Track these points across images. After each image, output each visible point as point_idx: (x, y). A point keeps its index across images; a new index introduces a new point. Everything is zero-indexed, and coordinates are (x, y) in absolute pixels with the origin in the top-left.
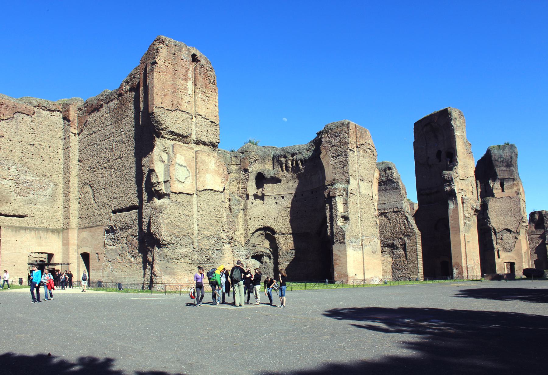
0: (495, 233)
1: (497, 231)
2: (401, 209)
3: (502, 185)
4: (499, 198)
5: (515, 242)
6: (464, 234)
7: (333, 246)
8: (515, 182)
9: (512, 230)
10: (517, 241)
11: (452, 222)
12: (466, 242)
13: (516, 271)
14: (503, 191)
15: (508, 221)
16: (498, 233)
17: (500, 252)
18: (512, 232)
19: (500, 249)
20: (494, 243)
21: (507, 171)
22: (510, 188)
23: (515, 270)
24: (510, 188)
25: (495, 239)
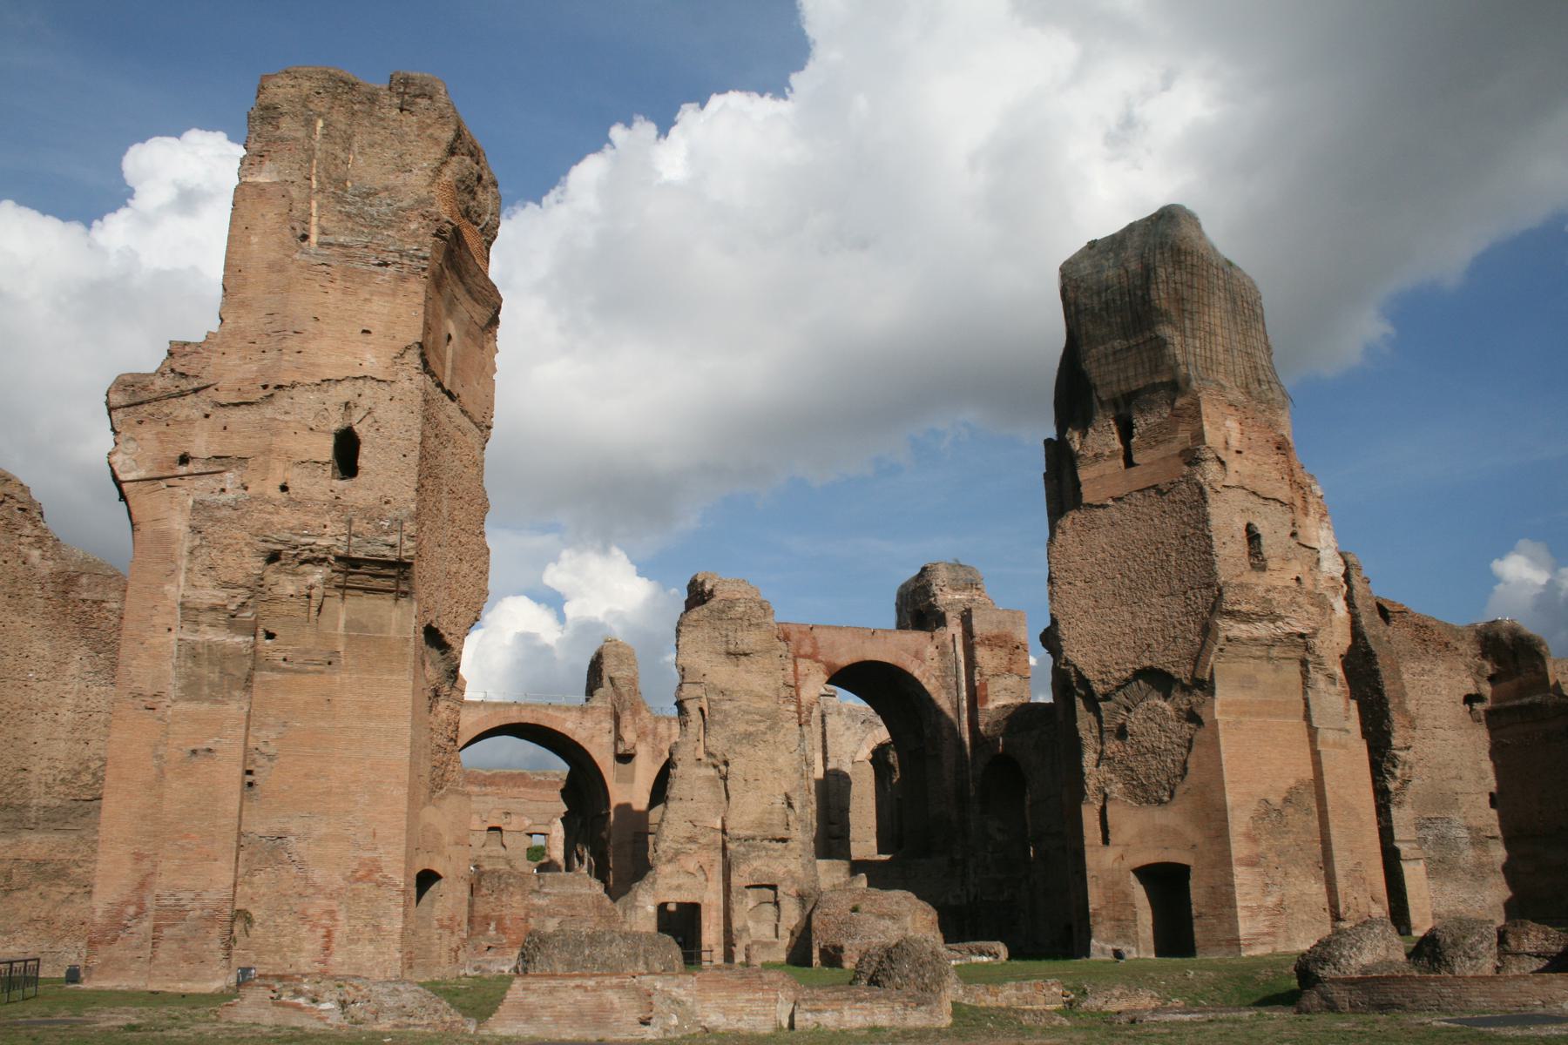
0: (1092, 703)
1: (1099, 688)
3: (1126, 432)
4: (1104, 506)
5: (1190, 741)
7: (566, 809)
9: (1173, 670)
10: (1200, 735)
13: (1200, 916)
14: (1129, 463)
15: (1154, 625)
16: (1107, 697)
18: (1178, 686)
20: (1089, 758)
21: (1134, 351)
22: (1157, 437)
23: (1194, 912)
24: (1160, 439)
25: (1095, 732)
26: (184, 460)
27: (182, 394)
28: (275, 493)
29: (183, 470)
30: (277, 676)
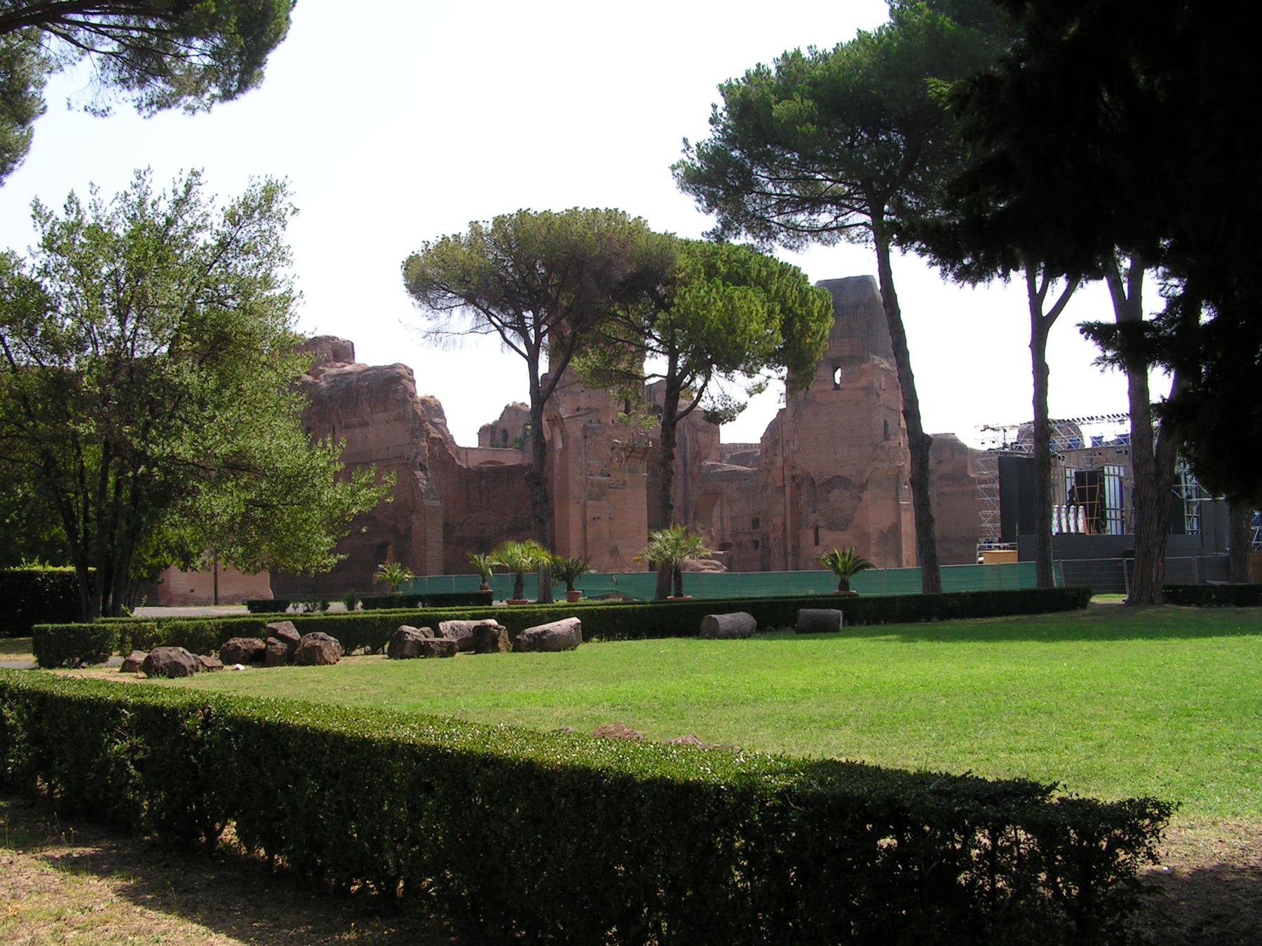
1: (817, 483)
2: (408, 459)
6: (585, 503)
8: (864, 366)
11: (559, 478)
12: (589, 518)
17: (820, 531)
19: (821, 523)
26: (578, 410)
27: (575, 382)
28: (610, 423)
29: (578, 413)
30: (611, 490)
